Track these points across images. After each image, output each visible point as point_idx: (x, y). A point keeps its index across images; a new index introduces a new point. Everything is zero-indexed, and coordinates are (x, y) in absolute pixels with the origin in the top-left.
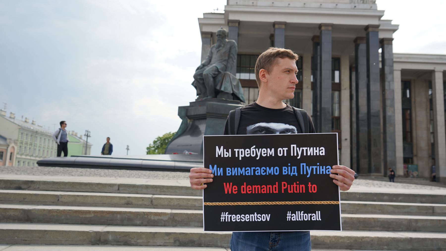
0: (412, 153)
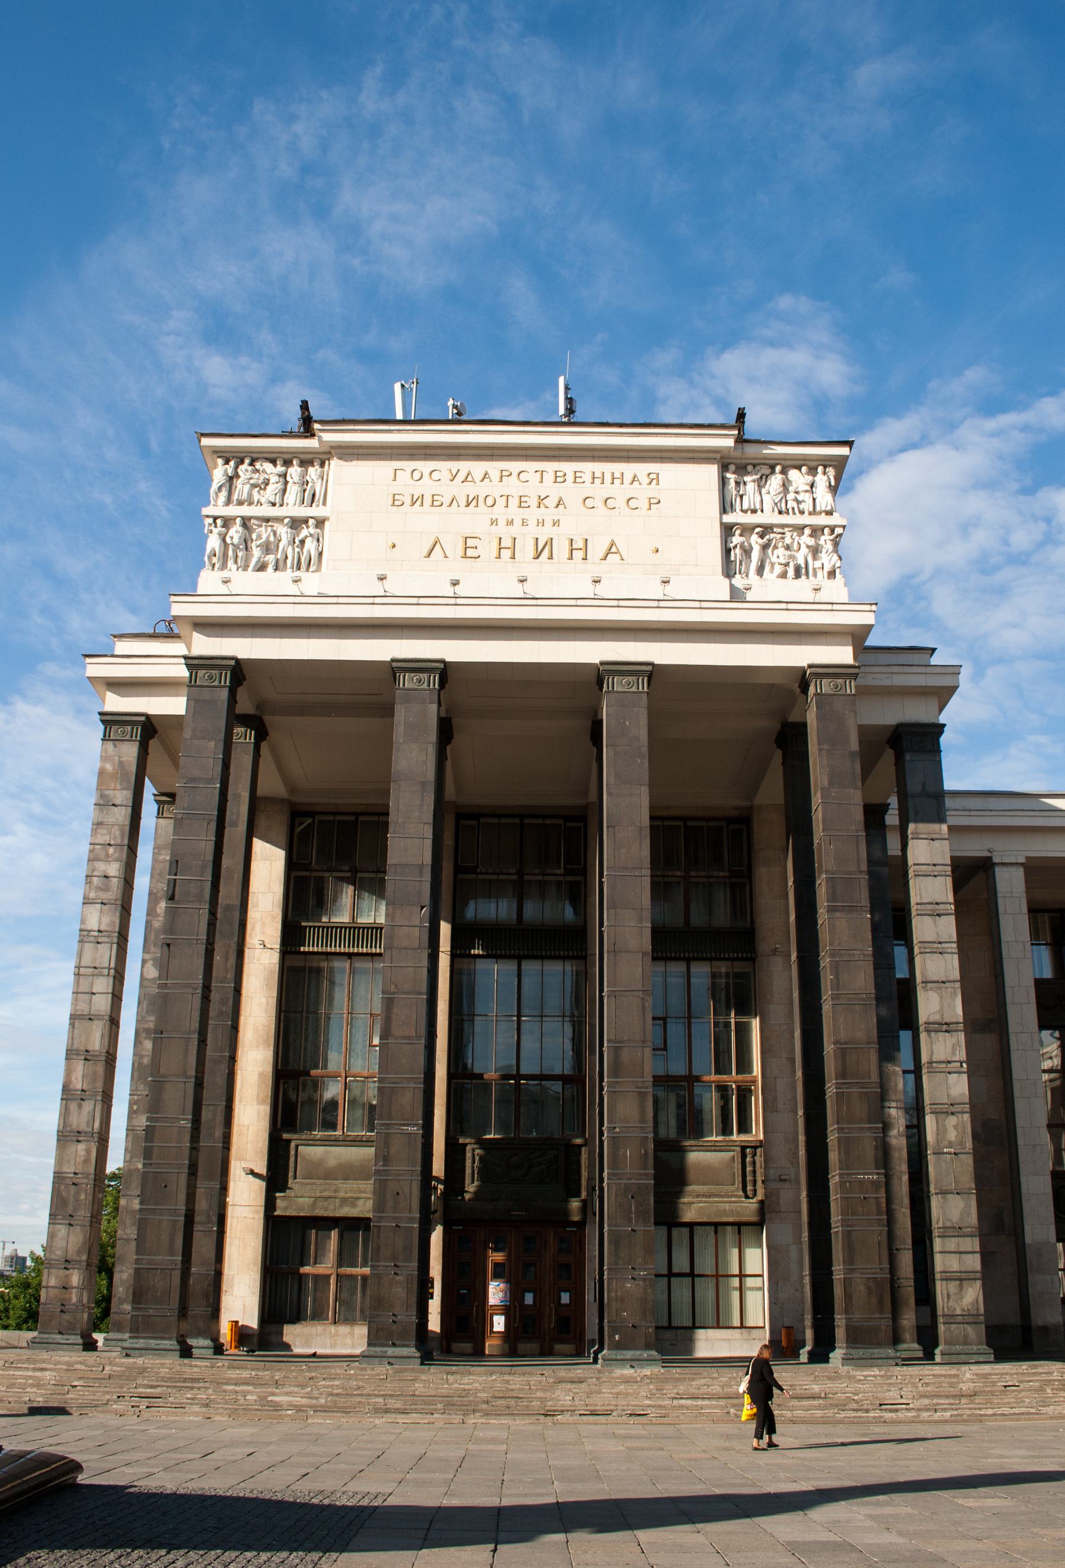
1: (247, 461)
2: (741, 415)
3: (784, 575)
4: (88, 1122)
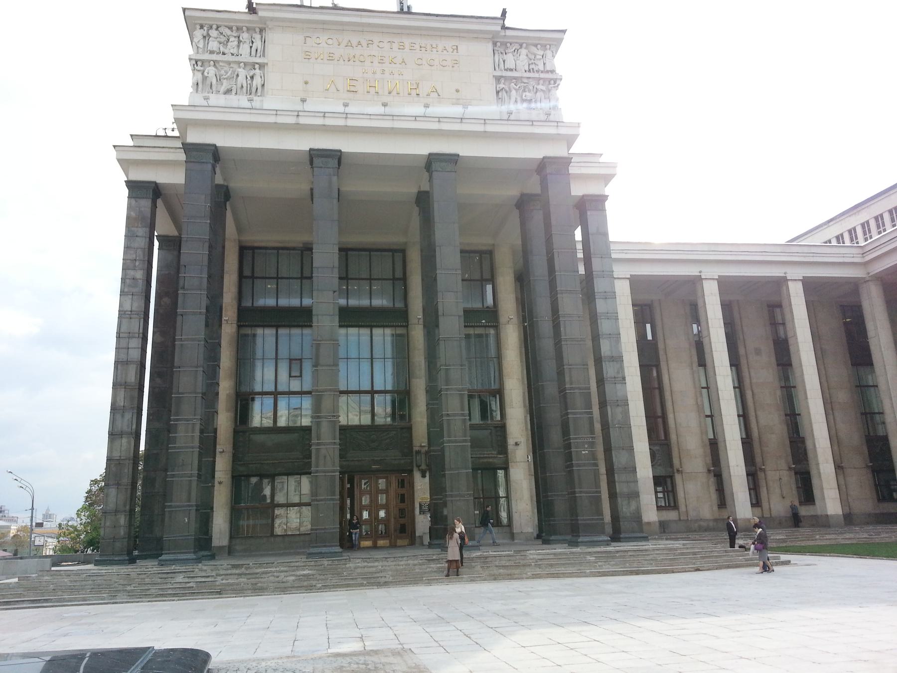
0: (671, 465)
1: (214, 27)
2: (504, 13)
4: (128, 426)
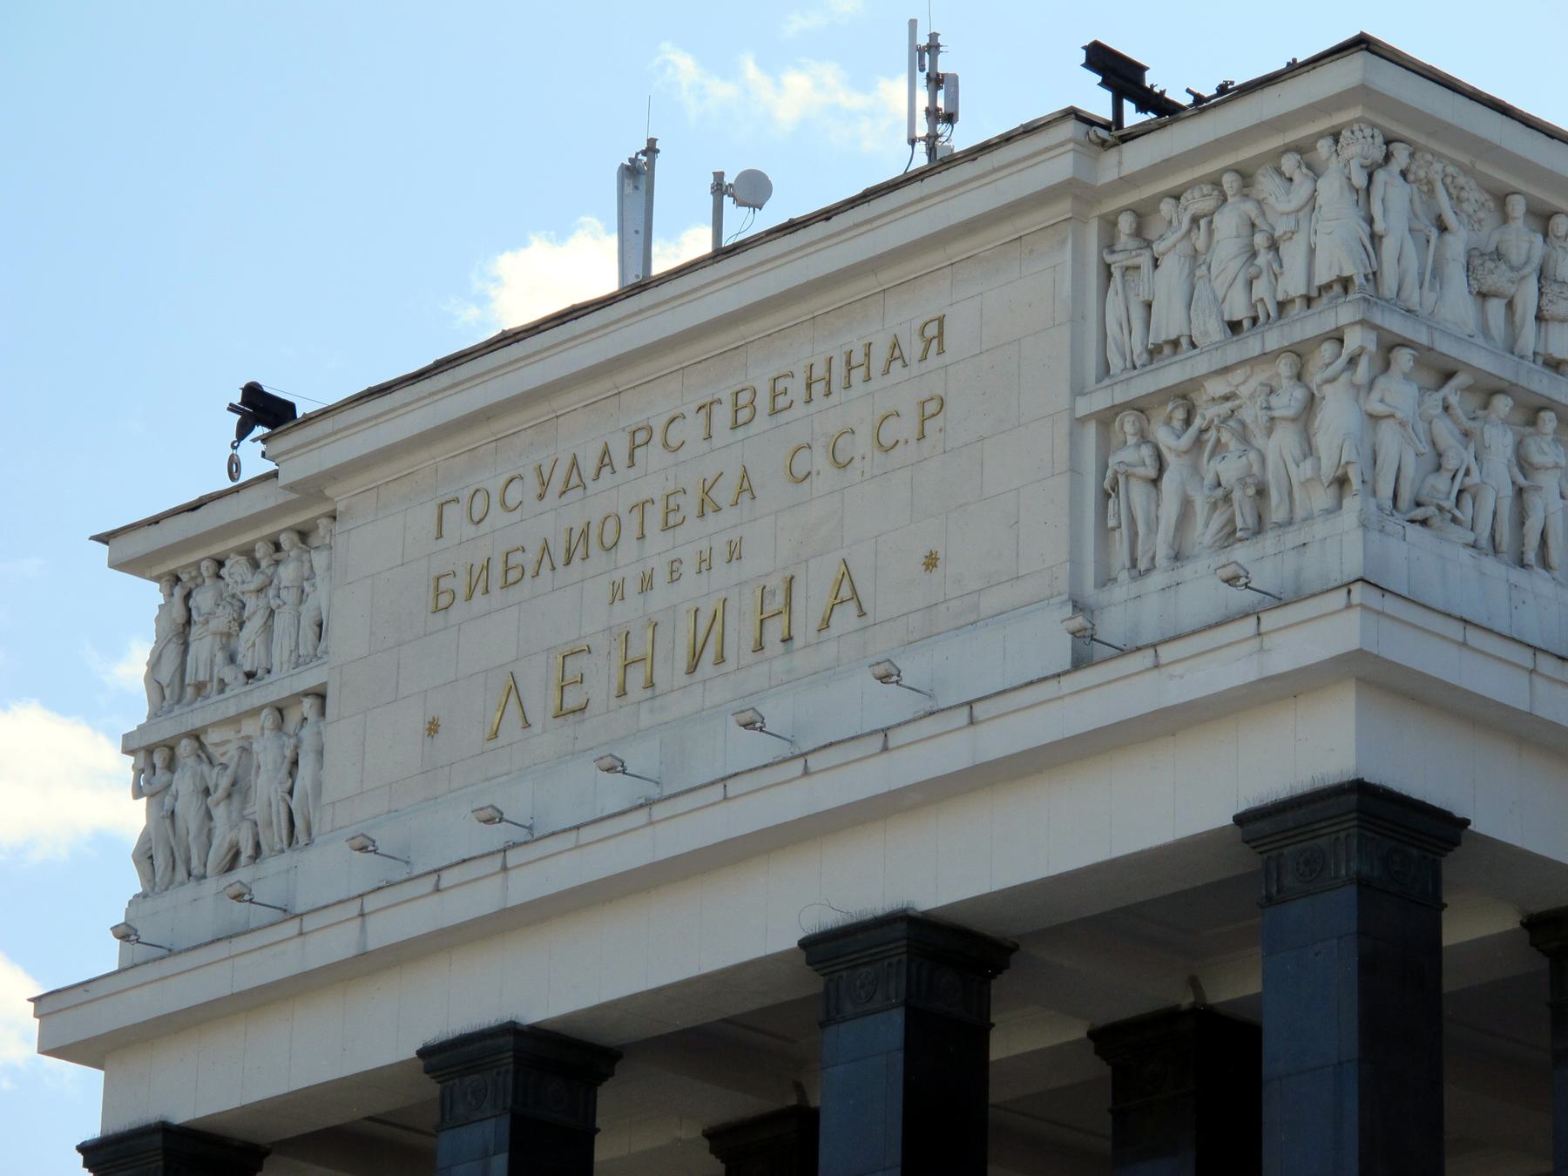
3: (1230, 535)
